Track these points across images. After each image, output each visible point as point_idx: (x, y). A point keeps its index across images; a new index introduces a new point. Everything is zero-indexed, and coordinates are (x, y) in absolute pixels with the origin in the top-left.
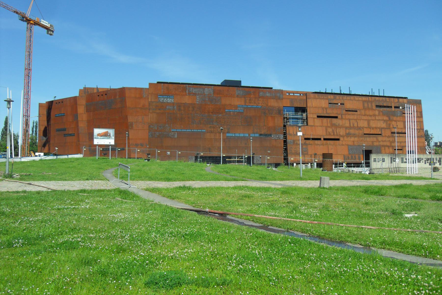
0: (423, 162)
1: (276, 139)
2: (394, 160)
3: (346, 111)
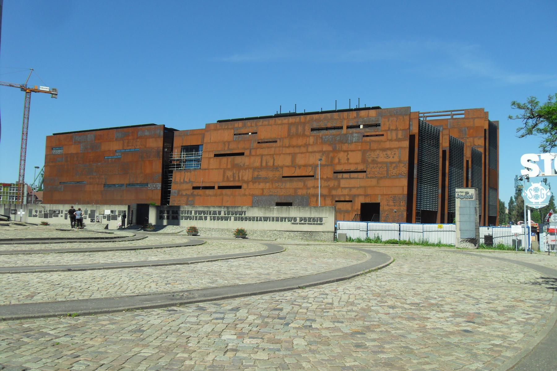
0: (62, 216)
1: (153, 189)
3: (259, 143)
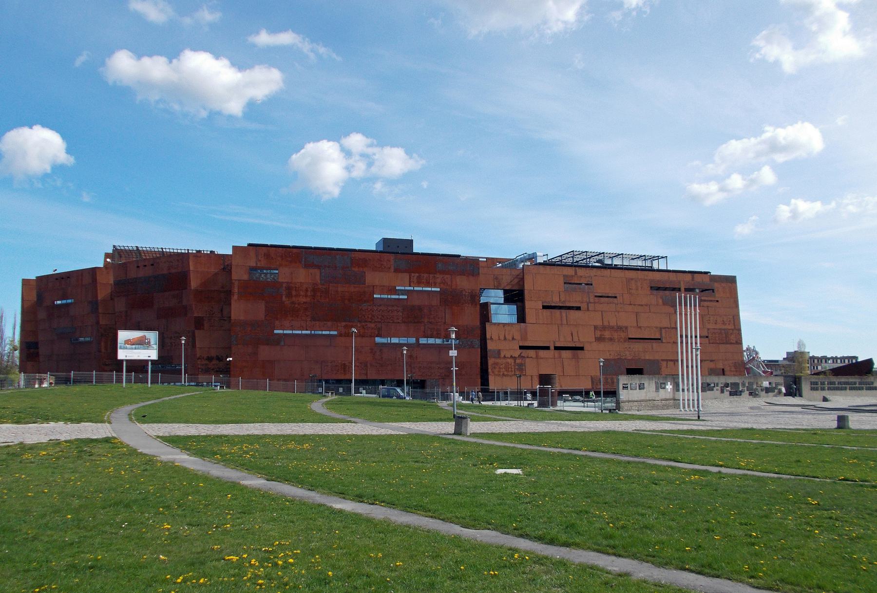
0: (717, 390)
2: (663, 386)
